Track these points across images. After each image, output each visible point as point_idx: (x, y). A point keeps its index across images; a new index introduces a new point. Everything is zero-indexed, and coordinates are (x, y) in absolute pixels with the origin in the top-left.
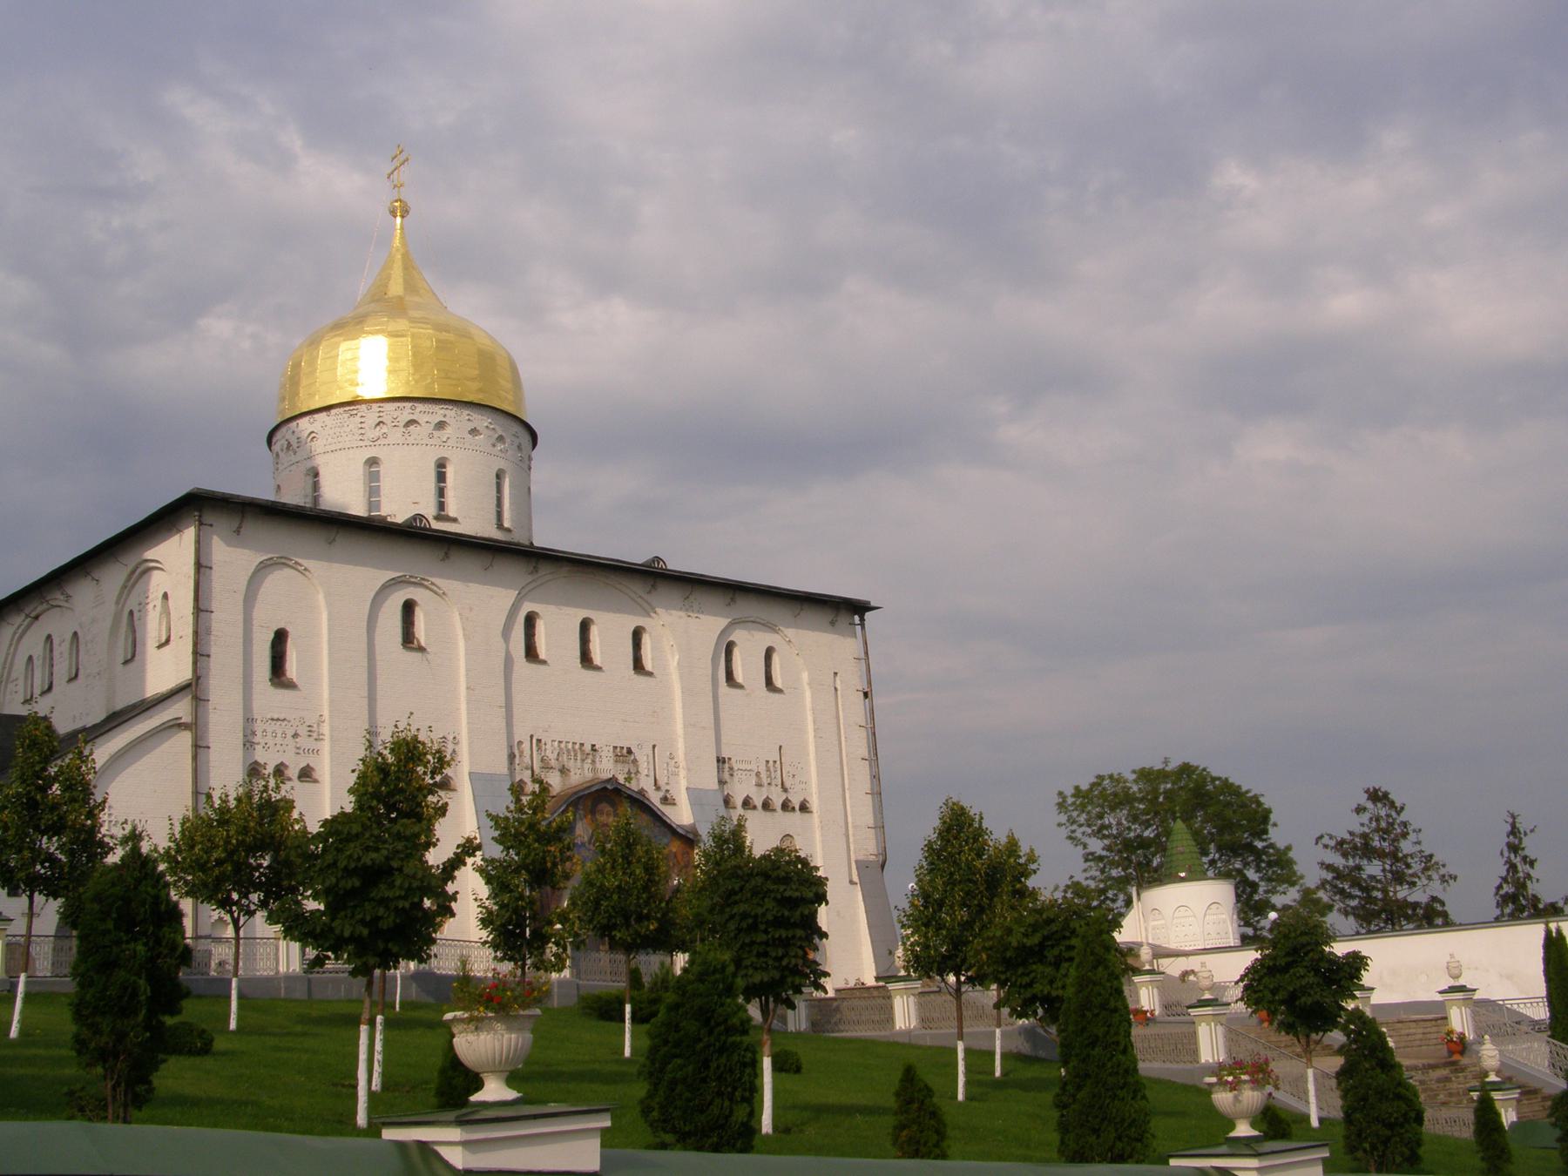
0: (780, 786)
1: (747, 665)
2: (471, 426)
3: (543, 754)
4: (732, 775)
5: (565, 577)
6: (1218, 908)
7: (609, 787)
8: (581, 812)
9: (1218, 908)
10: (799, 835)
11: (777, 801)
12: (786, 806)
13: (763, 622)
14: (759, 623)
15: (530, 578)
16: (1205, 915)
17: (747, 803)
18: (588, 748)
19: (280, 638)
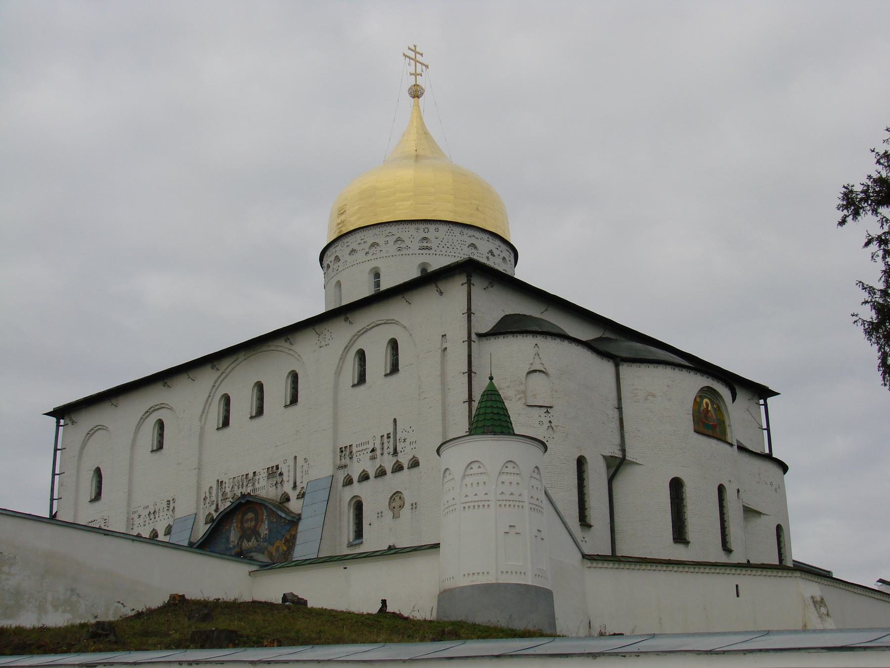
0: (392, 453)
1: (377, 362)
2: (350, 249)
3: (223, 490)
4: (351, 458)
5: (245, 360)
6: (479, 467)
7: (243, 501)
8: (235, 524)
9: (479, 467)
10: (406, 489)
11: (389, 468)
12: (398, 468)
13: (383, 322)
14: (382, 324)
15: (219, 373)
16: (464, 476)
17: (365, 477)
18: (251, 475)
19: (98, 472)
